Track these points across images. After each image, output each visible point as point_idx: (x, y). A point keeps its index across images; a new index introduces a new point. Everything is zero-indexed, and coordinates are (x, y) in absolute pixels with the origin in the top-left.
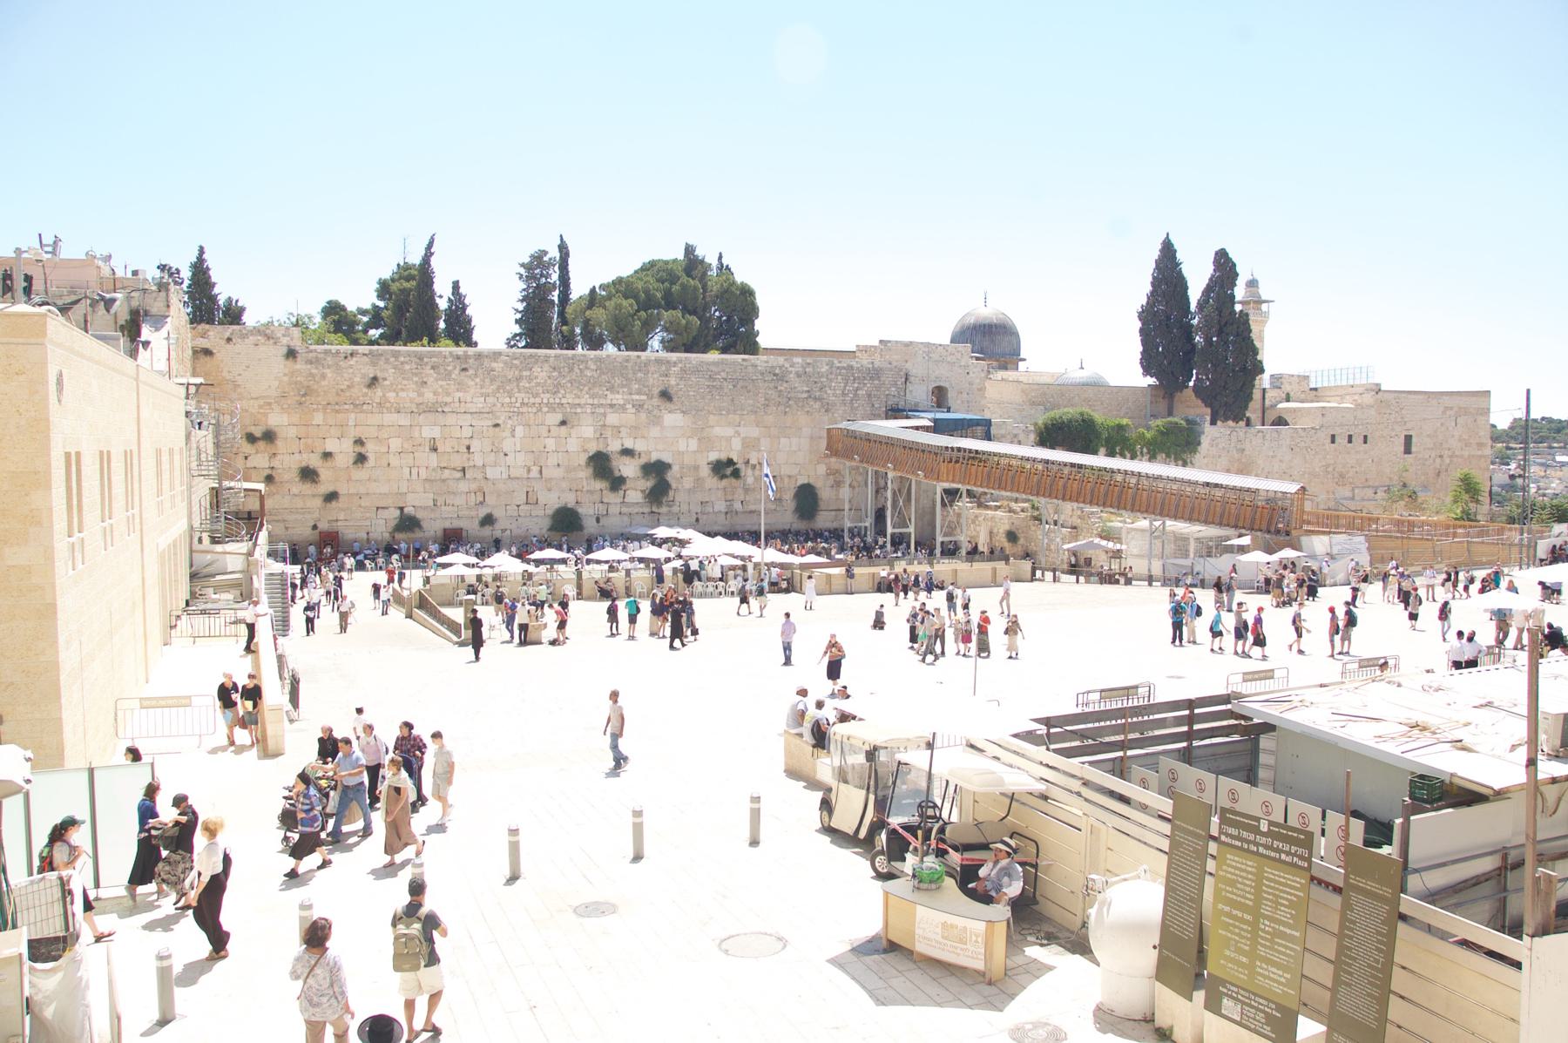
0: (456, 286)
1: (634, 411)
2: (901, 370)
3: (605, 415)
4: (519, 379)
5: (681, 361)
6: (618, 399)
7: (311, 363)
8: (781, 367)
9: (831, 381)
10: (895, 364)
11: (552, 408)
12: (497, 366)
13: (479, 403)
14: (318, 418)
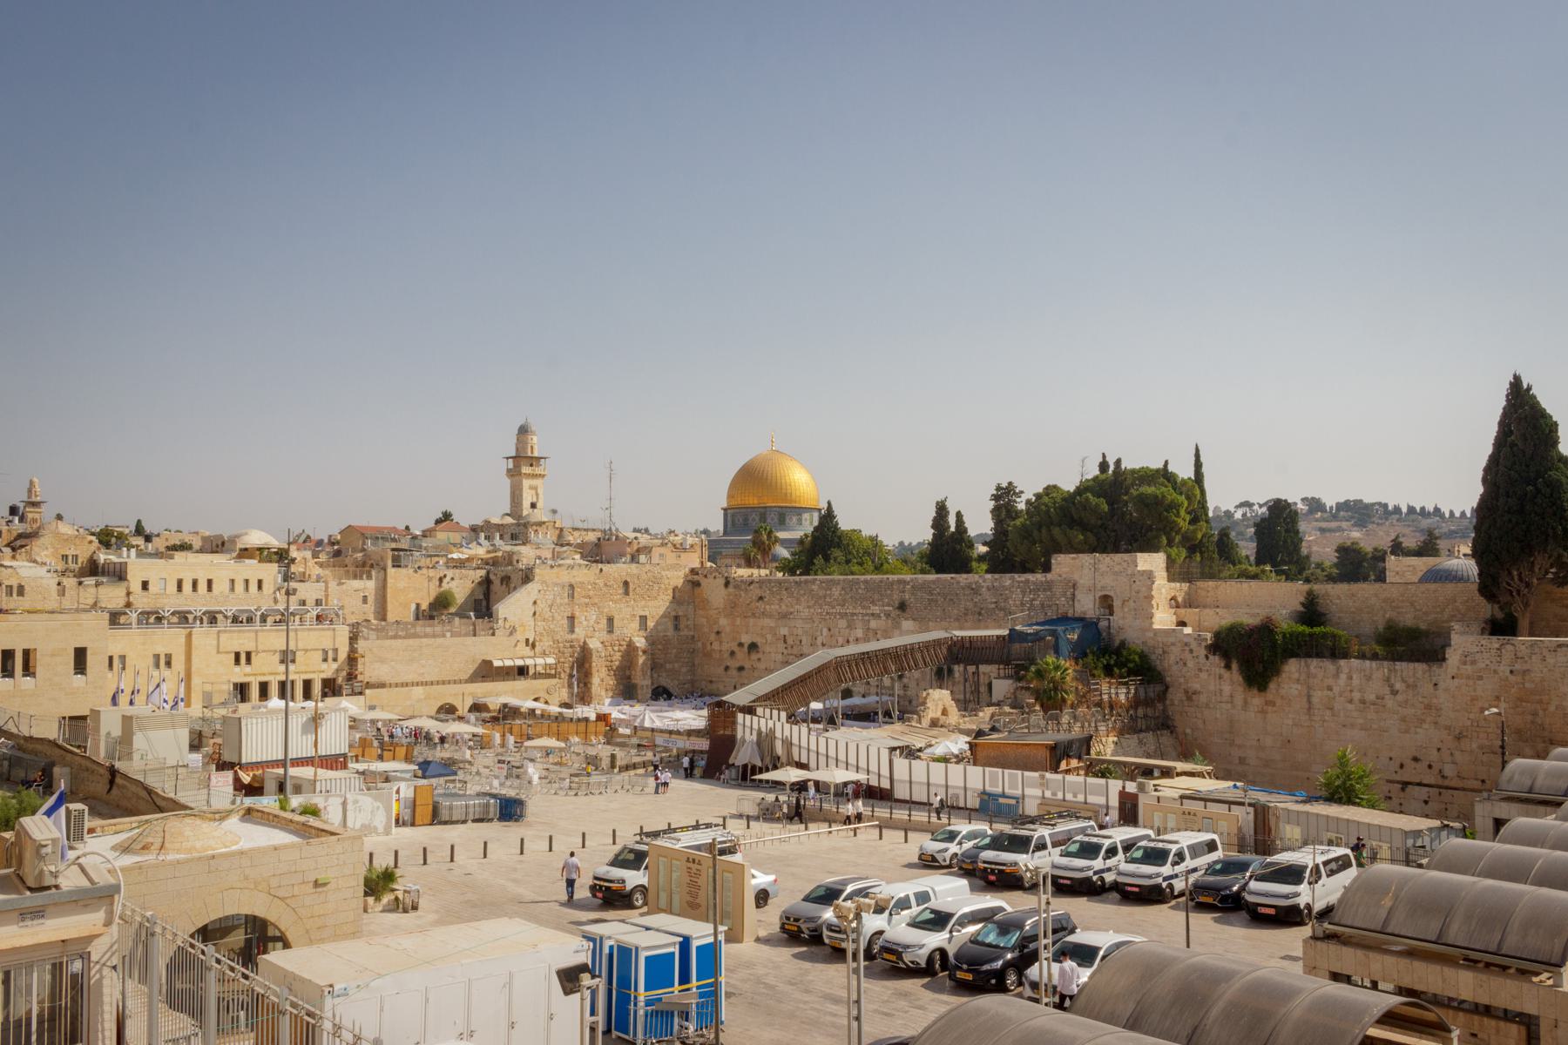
0: (959, 515)
1: (884, 618)
2: (1070, 581)
3: (869, 621)
4: (825, 597)
5: (912, 580)
6: (876, 609)
7: (735, 587)
8: (976, 583)
9: (1013, 592)
10: (1064, 576)
11: (843, 615)
12: (815, 587)
13: (806, 613)
14: (738, 621)
